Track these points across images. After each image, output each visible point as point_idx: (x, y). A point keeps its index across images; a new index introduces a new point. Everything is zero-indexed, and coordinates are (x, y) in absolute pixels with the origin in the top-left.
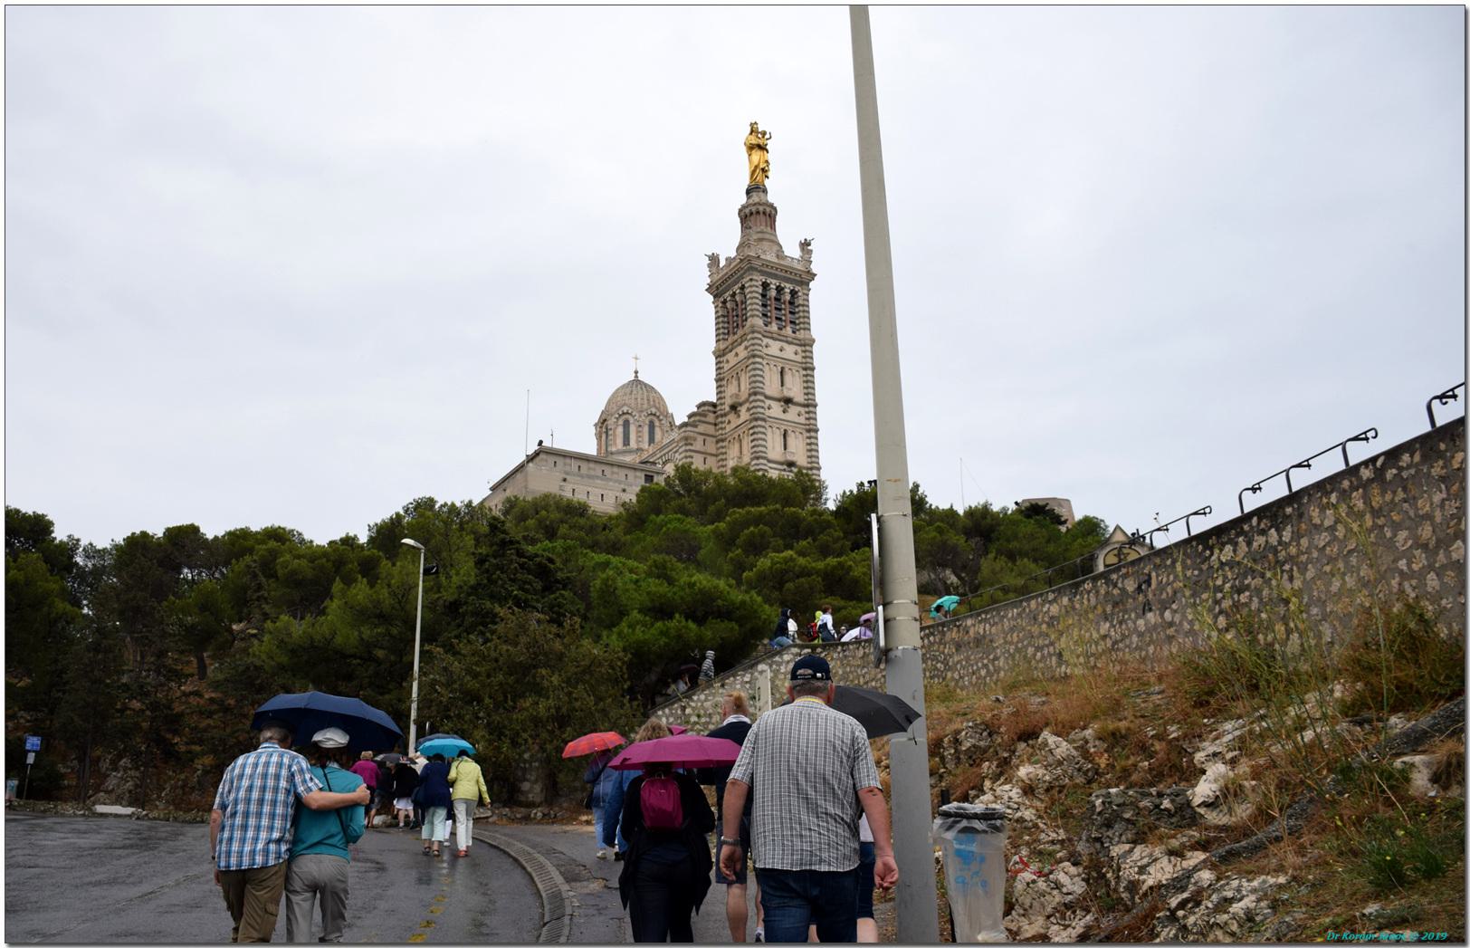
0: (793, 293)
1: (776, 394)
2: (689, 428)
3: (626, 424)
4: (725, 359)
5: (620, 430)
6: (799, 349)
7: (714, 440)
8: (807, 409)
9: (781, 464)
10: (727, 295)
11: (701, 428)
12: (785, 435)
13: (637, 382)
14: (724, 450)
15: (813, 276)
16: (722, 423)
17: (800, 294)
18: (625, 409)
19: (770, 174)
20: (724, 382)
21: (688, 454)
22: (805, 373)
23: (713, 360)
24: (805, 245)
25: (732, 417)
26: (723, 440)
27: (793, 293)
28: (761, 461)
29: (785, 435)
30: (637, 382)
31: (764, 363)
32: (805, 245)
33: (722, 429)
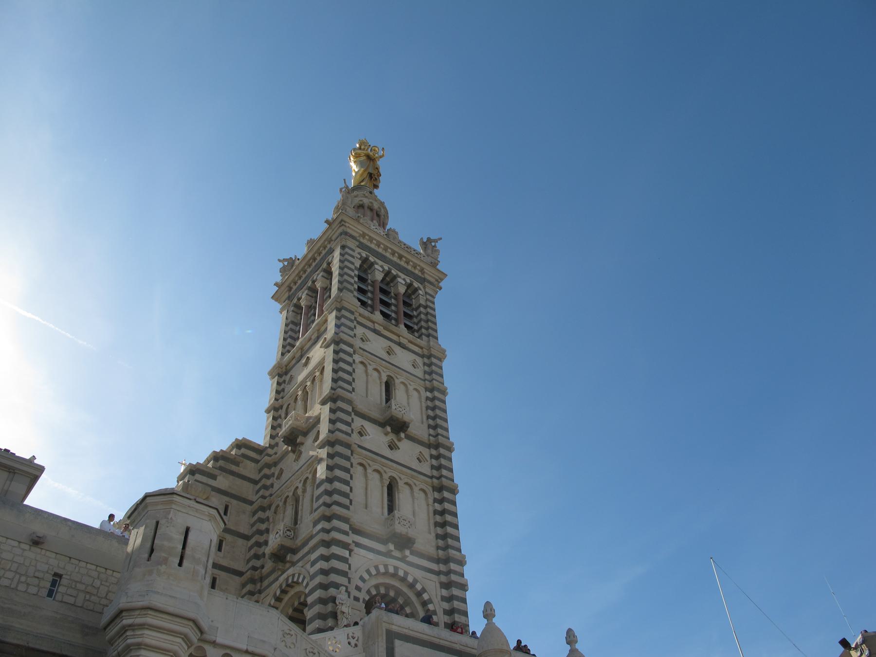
0: (411, 291)
1: (375, 415)
2: (198, 477)
6: (419, 361)
7: (249, 508)
8: (434, 452)
9: (384, 542)
11: (223, 482)
12: (391, 489)
14: (263, 527)
16: (267, 477)
17: (420, 292)
19: (380, 185)
20: (282, 413)
22: (429, 394)
26: (263, 509)
28: (336, 523)
29: (391, 489)
31: (358, 358)
33: (265, 487)
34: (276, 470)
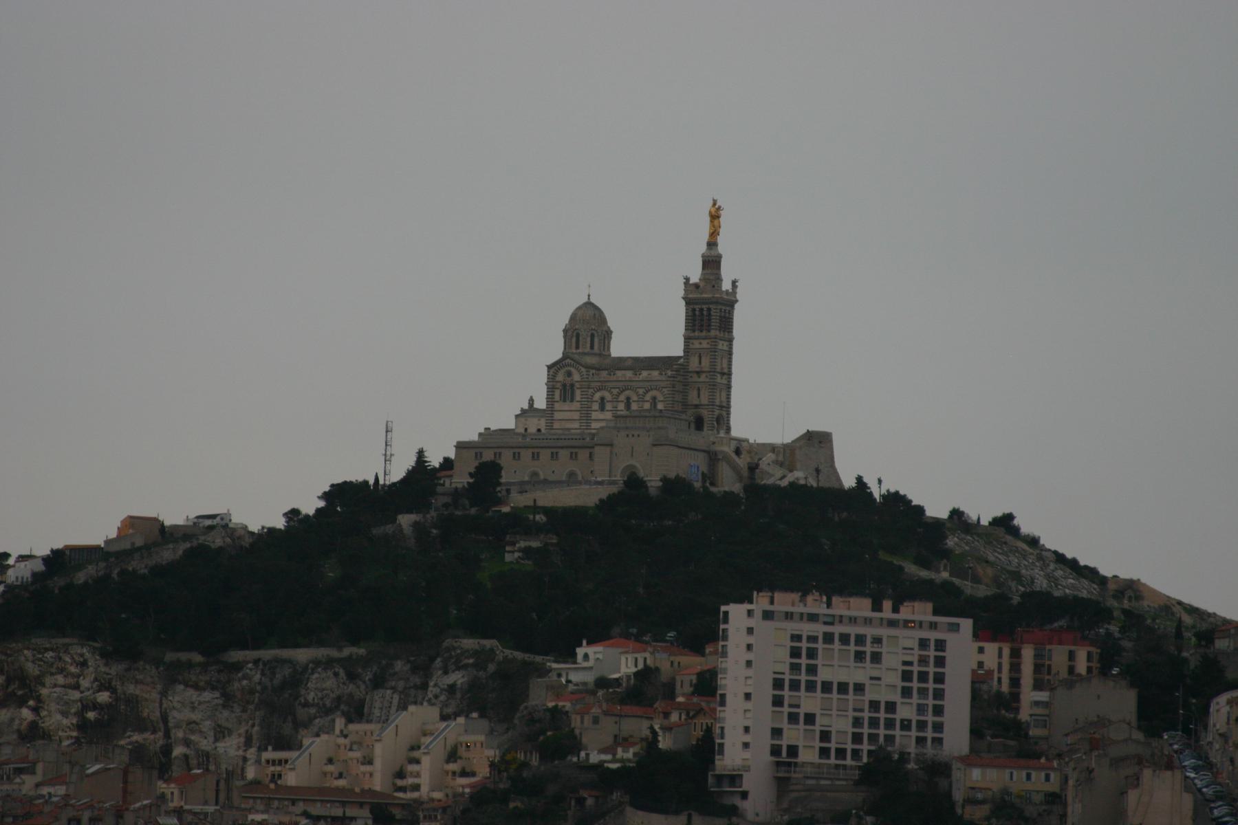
0: (729, 311)
3: (592, 336)
4: (691, 341)
5: (589, 339)
10: (697, 307)
13: (589, 305)
15: (737, 301)
18: (593, 327)
20: (690, 354)
21: (673, 392)
23: (682, 340)
24: (734, 283)
25: (695, 375)
27: (729, 311)
30: (589, 305)
32: (734, 283)
34: (690, 375)
